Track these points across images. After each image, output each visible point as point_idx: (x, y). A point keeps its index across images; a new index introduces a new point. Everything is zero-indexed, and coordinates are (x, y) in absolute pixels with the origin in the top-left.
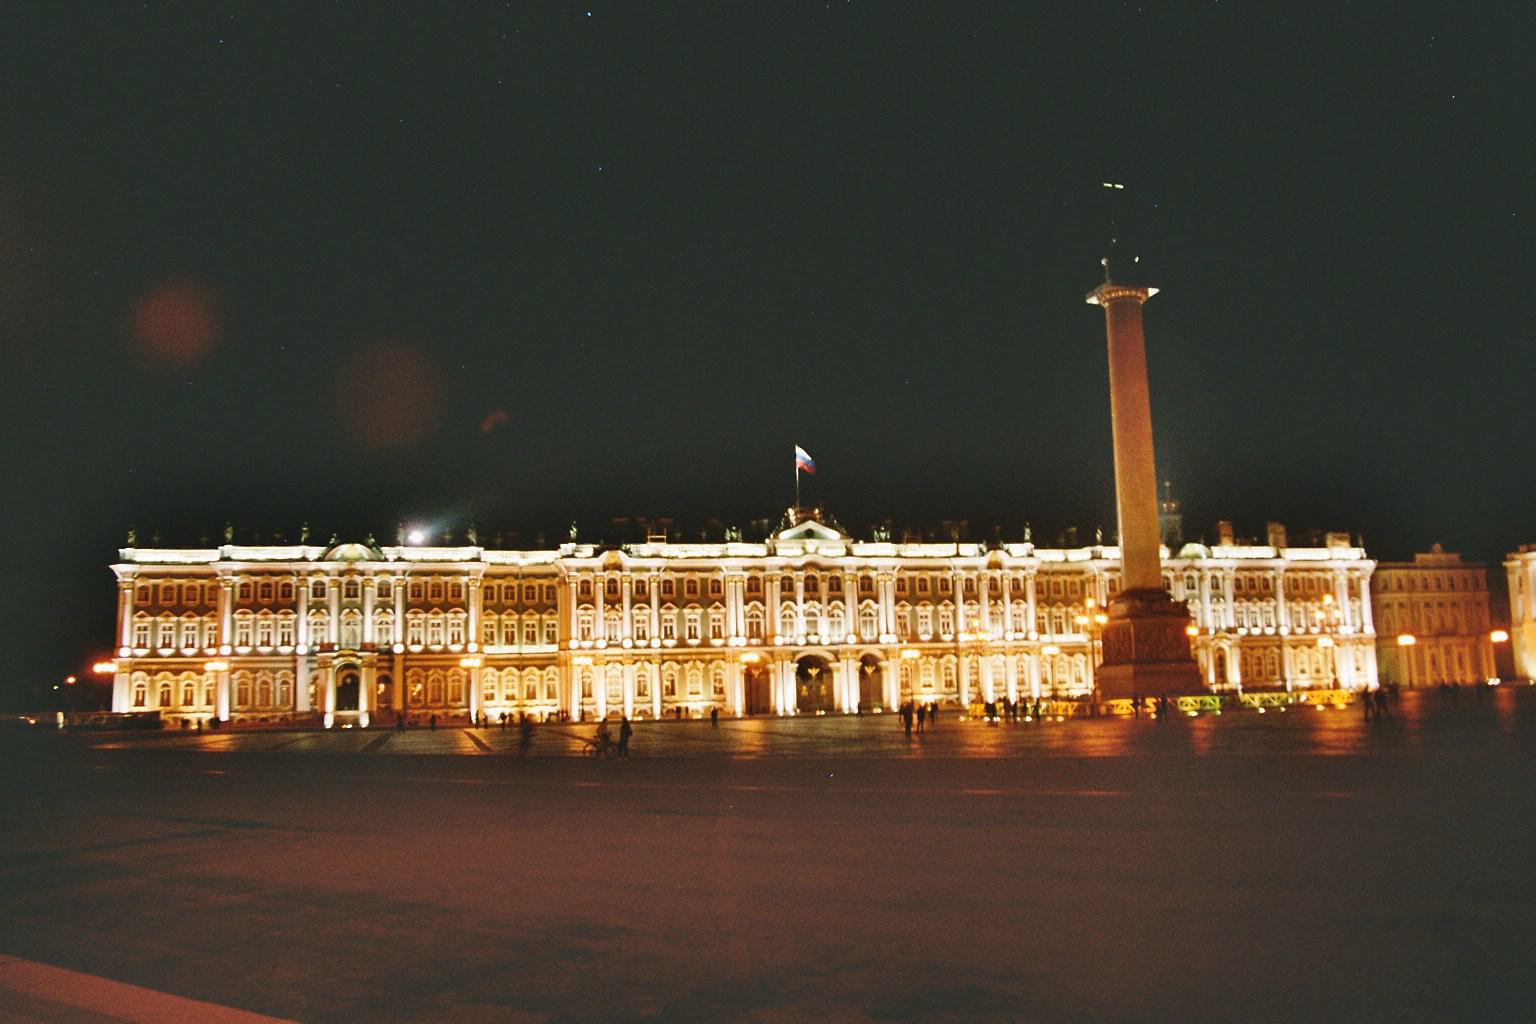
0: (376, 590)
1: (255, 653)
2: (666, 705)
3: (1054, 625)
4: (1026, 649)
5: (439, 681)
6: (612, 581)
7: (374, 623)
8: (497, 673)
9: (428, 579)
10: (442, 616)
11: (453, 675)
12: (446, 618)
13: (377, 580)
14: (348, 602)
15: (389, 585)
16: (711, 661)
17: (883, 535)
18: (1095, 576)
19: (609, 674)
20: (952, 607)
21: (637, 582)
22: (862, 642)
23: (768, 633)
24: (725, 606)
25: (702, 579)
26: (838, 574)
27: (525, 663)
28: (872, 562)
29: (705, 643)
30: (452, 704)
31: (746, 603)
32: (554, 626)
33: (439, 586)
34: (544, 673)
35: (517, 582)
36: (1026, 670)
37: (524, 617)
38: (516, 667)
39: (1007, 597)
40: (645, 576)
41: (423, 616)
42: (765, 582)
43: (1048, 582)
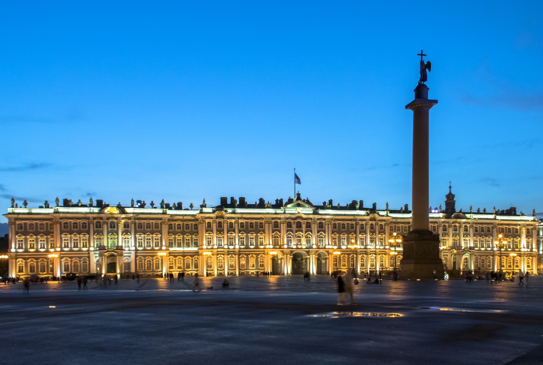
1: (71, 250)
6: (220, 223)
10: (151, 236)
16: (259, 254)
21: (230, 223)
22: (319, 248)
25: (255, 222)
26: (310, 221)
28: (324, 217)
29: (257, 247)
31: (273, 232)
32: (197, 240)
33: (150, 224)
37: (185, 236)
39: (377, 232)
40: (233, 221)
41: (143, 236)
43: (395, 226)
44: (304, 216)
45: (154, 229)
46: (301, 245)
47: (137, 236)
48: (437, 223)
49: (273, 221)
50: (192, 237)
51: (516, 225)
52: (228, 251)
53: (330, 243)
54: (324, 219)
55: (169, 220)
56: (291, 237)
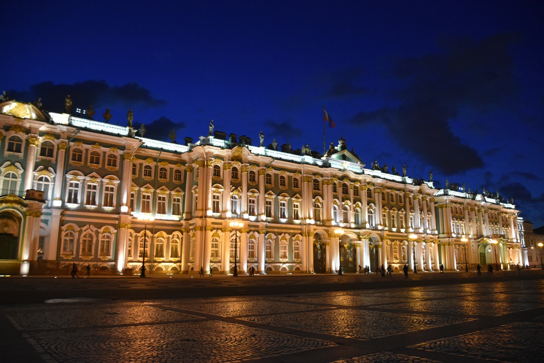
0: (39, 149)
5: (91, 236)
7: (34, 178)
8: (134, 234)
9: (89, 147)
11: (104, 232)
12: (102, 182)
13: (41, 139)
14: (10, 155)
15: (53, 146)
18: (446, 204)
24: (302, 197)
29: (290, 222)
30: (101, 257)
34: (171, 236)
35: (155, 163)
41: (81, 178)
42: (323, 184)
44: (353, 176)
45: (106, 167)
47: (69, 176)
49: (314, 177)
50: (170, 194)
51: (506, 213)
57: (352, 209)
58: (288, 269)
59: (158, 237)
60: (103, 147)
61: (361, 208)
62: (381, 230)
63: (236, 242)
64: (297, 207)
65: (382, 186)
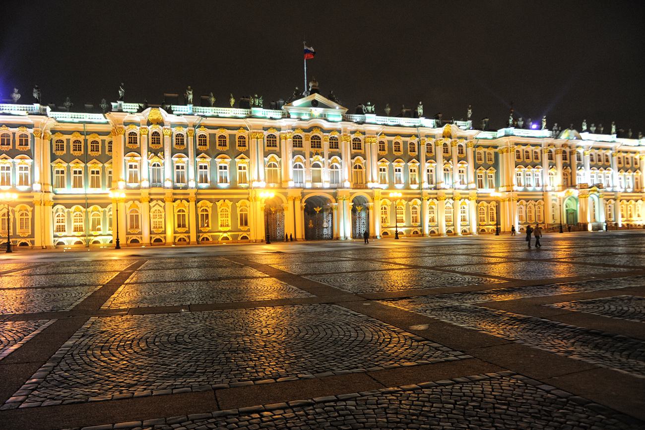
2: (201, 234)
3: (488, 181)
4: (467, 196)
8: (66, 210)
10: (10, 160)
12: (14, 163)
16: (238, 200)
17: (369, 108)
19: (153, 210)
20: (418, 164)
21: (177, 135)
23: (283, 179)
26: (336, 135)
27: (89, 201)
28: (362, 128)
29: (234, 187)
33: (8, 136)
35: (83, 137)
36: (467, 210)
37: (89, 165)
38: (84, 206)
39: (455, 159)
40: (183, 131)
42: (280, 139)
45: (17, 147)
46: (320, 181)
48: (540, 145)
49: (266, 133)
52: (174, 194)
53: (375, 178)
54: (364, 133)
55: (54, 132)
56: (300, 167)
57: (326, 166)
58: (230, 239)
59: (92, 211)
60: (11, 128)
61: (341, 164)
62: (371, 189)
63: (8, 215)
64: (244, 168)
65: (377, 134)
